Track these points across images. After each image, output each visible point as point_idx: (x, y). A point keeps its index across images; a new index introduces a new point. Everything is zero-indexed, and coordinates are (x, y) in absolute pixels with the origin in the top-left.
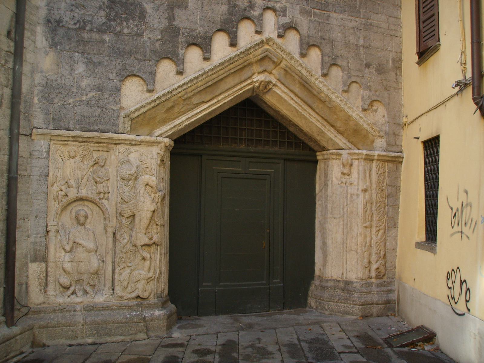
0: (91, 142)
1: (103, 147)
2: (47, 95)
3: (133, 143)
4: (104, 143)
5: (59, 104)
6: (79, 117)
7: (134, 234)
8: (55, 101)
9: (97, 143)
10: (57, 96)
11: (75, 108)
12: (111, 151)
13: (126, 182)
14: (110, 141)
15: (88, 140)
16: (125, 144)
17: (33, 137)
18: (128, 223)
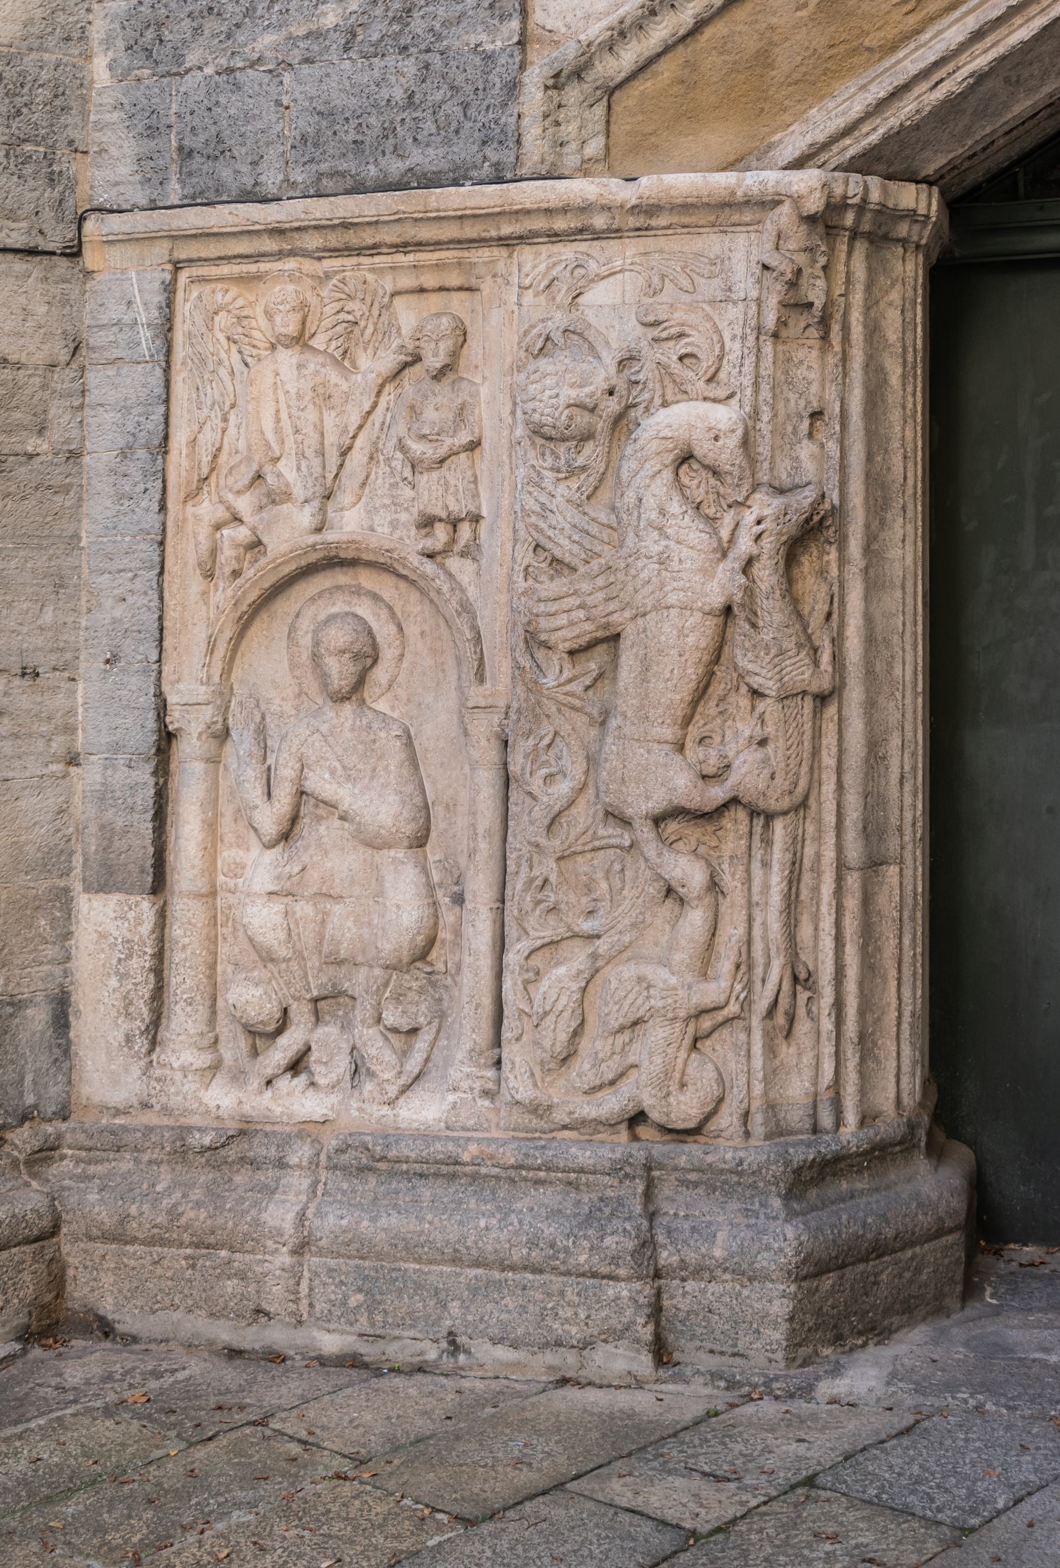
0: (374, 249)
1: (439, 266)
2: (150, 34)
3: (599, 222)
4: (437, 245)
5: (209, 71)
6: (306, 123)
7: (611, 746)
8: (192, 59)
9: (403, 247)
10: (198, 31)
11: (287, 77)
12: (487, 287)
13: (562, 449)
14: (470, 231)
15: (352, 238)
16: (555, 237)
17: (90, 258)
18: (576, 687)
